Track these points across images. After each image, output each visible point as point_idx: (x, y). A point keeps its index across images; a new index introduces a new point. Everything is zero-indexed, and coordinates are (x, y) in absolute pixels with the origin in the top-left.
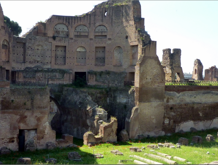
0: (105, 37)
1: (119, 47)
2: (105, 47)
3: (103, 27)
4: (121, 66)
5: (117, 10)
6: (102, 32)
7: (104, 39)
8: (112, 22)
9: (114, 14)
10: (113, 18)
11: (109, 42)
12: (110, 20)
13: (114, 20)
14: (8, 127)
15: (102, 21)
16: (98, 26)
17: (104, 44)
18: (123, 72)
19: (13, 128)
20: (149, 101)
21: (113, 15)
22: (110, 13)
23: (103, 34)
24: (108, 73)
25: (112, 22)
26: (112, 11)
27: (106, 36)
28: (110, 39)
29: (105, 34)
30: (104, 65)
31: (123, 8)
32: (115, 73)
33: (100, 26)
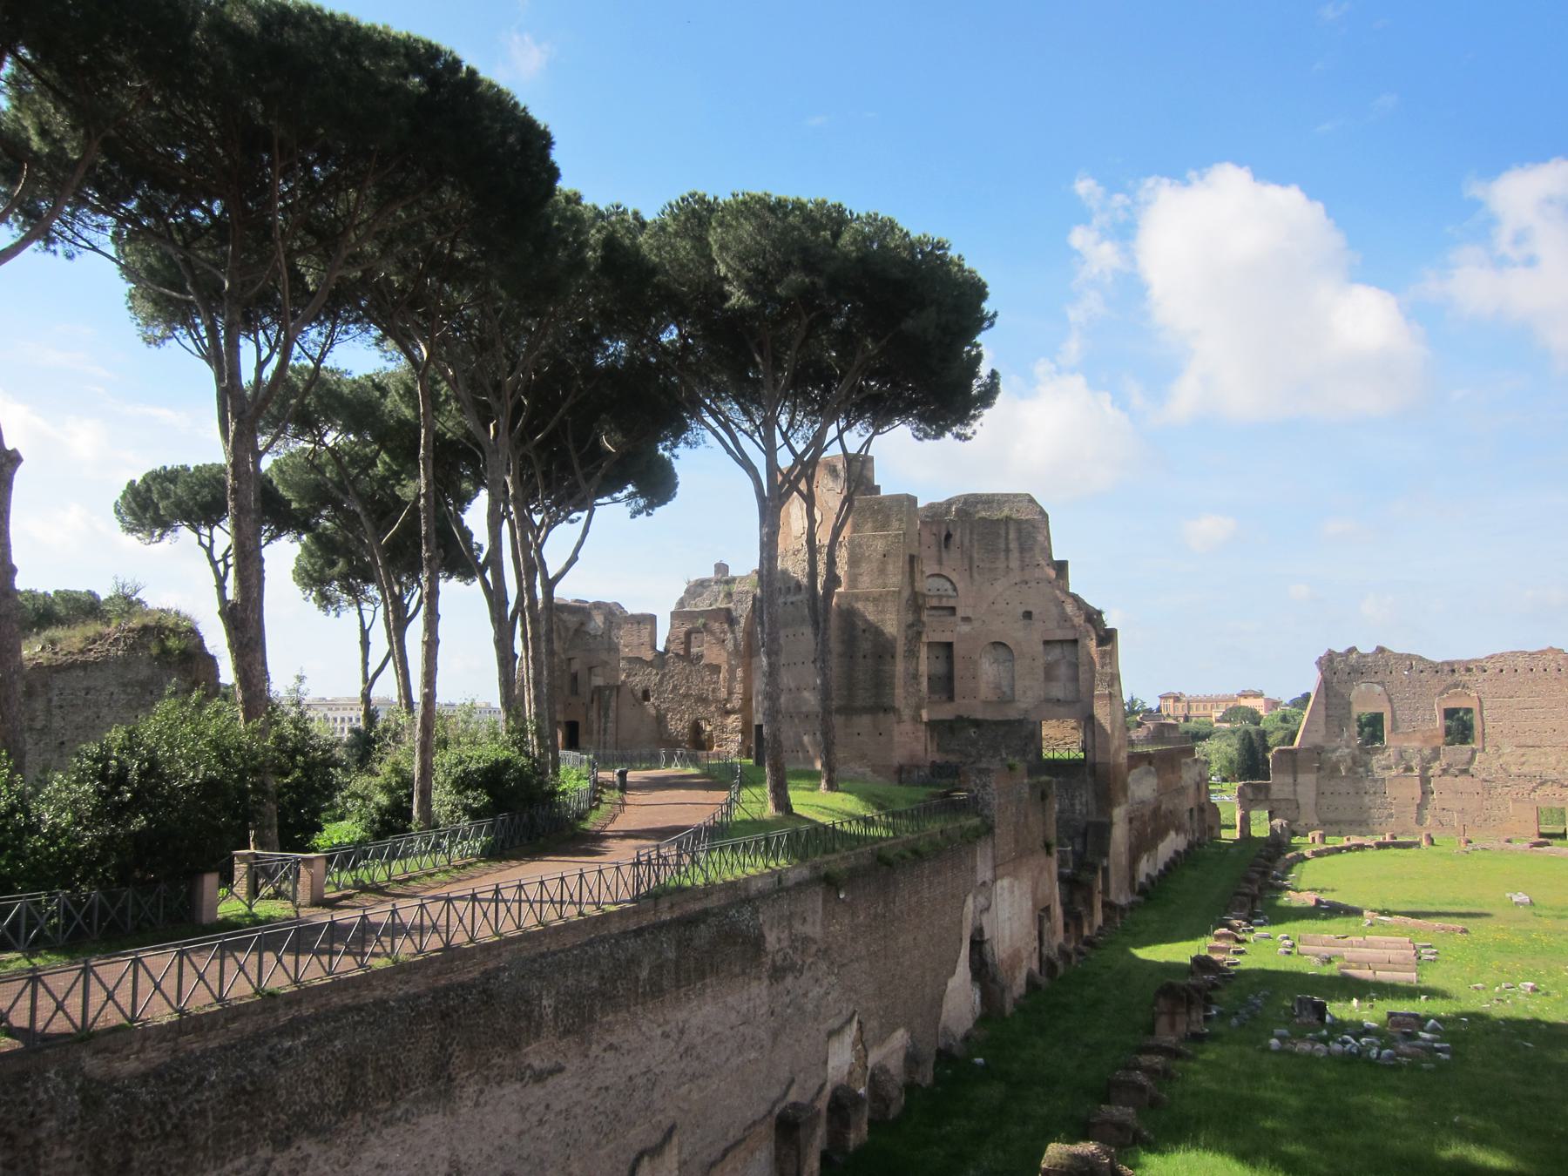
0: (945, 612)
1: (995, 644)
2: (949, 645)
3: (942, 581)
4: (1005, 700)
6: (940, 597)
7: (952, 619)
8: (971, 568)
9: (976, 544)
12: (966, 561)
13: (976, 563)
15: (940, 562)
16: (933, 575)
17: (948, 634)
18: (1020, 722)
19: (1035, 905)
20: (1119, 805)
21: (972, 546)
22: (962, 544)
23: (945, 603)
24: (977, 724)
25: (971, 568)
26: (971, 533)
27: (952, 610)
28: (967, 619)
29: (951, 603)
30: (951, 698)
33: (933, 575)
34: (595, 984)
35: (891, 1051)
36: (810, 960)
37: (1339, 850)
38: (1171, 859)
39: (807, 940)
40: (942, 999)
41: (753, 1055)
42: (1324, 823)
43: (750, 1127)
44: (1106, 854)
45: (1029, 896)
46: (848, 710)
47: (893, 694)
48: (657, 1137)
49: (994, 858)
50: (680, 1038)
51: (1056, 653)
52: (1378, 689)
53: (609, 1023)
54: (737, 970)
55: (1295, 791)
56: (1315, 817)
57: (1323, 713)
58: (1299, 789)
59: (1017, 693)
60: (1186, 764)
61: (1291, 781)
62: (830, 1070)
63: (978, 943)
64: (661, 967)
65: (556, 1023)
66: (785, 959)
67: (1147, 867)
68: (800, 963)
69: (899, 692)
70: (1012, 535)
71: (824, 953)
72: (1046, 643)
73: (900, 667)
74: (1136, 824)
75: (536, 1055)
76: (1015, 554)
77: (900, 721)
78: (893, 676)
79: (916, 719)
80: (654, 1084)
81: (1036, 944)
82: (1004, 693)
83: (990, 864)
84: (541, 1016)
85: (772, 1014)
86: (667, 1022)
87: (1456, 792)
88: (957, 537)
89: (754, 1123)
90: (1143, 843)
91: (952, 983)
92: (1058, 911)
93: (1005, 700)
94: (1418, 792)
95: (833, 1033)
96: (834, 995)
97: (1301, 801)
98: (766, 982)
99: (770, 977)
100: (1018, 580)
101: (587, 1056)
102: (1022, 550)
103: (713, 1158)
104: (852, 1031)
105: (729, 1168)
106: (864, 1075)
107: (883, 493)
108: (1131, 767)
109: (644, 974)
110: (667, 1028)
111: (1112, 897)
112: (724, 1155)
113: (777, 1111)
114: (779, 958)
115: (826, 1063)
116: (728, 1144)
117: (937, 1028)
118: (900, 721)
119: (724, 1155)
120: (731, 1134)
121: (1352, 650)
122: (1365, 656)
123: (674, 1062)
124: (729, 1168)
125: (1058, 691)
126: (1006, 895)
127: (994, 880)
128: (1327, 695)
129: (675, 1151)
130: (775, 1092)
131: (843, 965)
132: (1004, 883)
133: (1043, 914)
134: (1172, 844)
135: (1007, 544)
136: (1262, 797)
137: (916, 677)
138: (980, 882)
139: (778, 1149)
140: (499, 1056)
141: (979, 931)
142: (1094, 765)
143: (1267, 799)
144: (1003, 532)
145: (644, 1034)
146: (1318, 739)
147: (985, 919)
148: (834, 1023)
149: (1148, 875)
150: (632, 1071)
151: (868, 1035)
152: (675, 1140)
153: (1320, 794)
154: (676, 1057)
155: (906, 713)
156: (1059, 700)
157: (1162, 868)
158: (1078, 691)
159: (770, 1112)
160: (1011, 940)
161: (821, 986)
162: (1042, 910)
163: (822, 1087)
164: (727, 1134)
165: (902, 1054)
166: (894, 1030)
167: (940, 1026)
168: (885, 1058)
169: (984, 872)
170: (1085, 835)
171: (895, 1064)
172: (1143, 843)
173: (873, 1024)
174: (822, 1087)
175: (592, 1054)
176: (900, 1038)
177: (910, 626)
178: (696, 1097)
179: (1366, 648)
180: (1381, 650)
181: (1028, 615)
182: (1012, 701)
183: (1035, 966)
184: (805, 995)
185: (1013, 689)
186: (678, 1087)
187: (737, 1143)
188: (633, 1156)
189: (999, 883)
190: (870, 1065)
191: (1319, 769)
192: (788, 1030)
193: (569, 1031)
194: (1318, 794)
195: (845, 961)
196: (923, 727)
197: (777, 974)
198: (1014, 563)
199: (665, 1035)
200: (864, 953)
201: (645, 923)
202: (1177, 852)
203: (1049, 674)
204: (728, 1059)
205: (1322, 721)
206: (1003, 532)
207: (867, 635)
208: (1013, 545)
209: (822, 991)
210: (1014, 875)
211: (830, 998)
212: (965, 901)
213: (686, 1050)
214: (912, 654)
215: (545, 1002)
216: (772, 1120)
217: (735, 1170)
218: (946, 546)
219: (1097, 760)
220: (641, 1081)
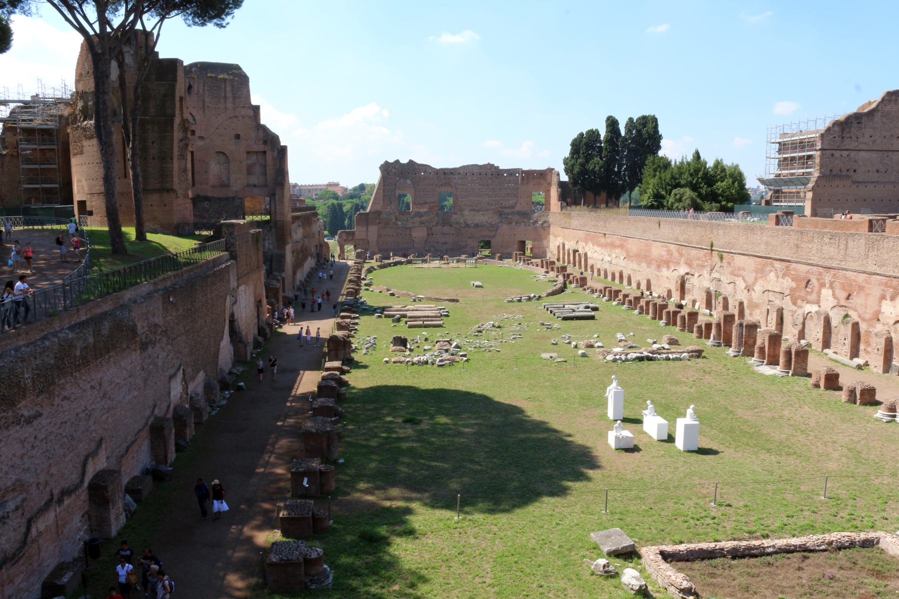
1: (217, 152)
4: (225, 185)
5: (212, 85)
8: (204, 107)
9: (206, 92)
10: (206, 99)
11: (201, 143)
14: (253, 298)
18: (234, 198)
19: (255, 299)
20: (288, 243)
21: (204, 94)
26: (204, 86)
28: (201, 138)
31: (225, 85)
32: (220, 199)
34: (52, 361)
35: (197, 385)
36: (158, 338)
37: (389, 265)
38: (309, 272)
39: (156, 325)
40: (218, 354)
41: (136, 393)
42: (380, 251)
43: (137, 433)
44: (283, 271)
45: (253, 294)
46: (146, 191)
47: (173, 181)
48: (93, 445)
49: (238, 275)
50: (100, 388)
51: (254, 158)
52: (409, 182)
53: (63, 384)
54: (124, 346)
55: (367, 236)
56: (376, 248)
57: (382, 194)
58: (369, 233)
59: (231, 181)
60: (314, 221)
61: (365, 229)
62: (172, 397)
63: (232, 321)
64: (86, 348)
65: (34, 387)
66: (146, 338)
67: (301, 276)
68: (154, 339)
69: (176, 180)
70: (228, 89)
71: (165, 332)
72: (248, 153)
73: (176, 165)
74: (295, 253)
75: (25, 408)
76: (231, 100)
77: (177, 197)
78: (172, 171)
79: (186, 196)
80: (89, 416)
81: (256, 320)
82: (224, 182)
83: (236, 278)
84: (25, 384)
85: (143, 369)
86: (93, 380)
87: (443, 234)
88: (195, 88)
89: (140, 431)
90: (298, 265)
91: (222, 345)
92: (265, 301)
93: (225, 185)
94: (425, 234)
95: (172, 377)
96: (171, 356)
97: (370, 240)
98: (139, 352)
99: (140, 349)
100: (232, 116)
101: (53, 405)
102: (234, 98)
103: (121, 453)
104: (180, 375)
105: (131, 456)
106: (187, 398)
107: (161, 56)
108: (293, 223)
109: (78, 353)
110: (93, 384)
111: (286, 294)
112: (127, 451)
113: (150, 423)
114: (143, 337)
115: (169, 393)
116: (128, 444)
117: (217, 369)
118: (177, 197)
119: (127, 451)
120: (129, 439)
121: (397, 162)
122: (404, 164)
123: (98, 403)
124: (131, 456)
125: (254, 180)
126: (243, 294)
127: (238, 287)
128: (384, 185)
129: (104, 452)
130: (148, 413)
131: (174, 339)
132: (242, 288)
133: (258, 304)
134: (310, 263)
135: (225, 94)
136: (351, 238)
137: (185, 170)
138: (232, 288)
139: (152, 443)
140: (4, 412)
141: (232, 315)
142: (276, 222)
143: (353, 239)
144: (223, 87)
145: (81, 388)
146: (378, 207)
147: (235, 307)
148: (172, 371)
149: (301, 281)
150: (78, 411)
151: (187, 377)
152: (104, 446)
153: (379, 236)
154: (99, 399)
155: (180, 192)
156: (255, 186)
157: (305, 276)
158: (266, 181)
159: (146, 424)
160: (246, 317)
161: (164, 352)
162: (258, 302)
163: (169, 407)
164: (127, 439)
165: (202, 385)
166: (199, 372)
167: (218, 368)
168: (196, 387)
169: (233, 283)
170: (271, 261)
171: (200, 390)
172: (298, 265)
173: (189, 370)
174: (169, 407)
175: (56, 403)
176: (201, 376)
177: (181, 140)
178: (111, 421)
179: (404, 161)
180: (411, 162)
181: (238, 137)
182: (228, 186)
183: (256, 332)
184: (158, 357)
185: (229, 179)
186: (101, 416)
187: (133, 443)
188: (82, 458)
189: (240, 288)
190: (189, 393)
191: (379, 223)
192: (151, 378)
193: (42, 392)
194: (378, 236)
195: (175, 336)
196: (190, 201)
197: (144, 347)
198: (230, 106)
199: (92, 388)
200: (183, 331)
201: (73, 323)
202: (311, 268)
203: (249, 172)
204: (124, 397)
205: (381, 198)
206: (223, 87)
207: (155, 145)
208: (229, 95)
209: (165, 354)
210: (245, 283)
211: (169, 357)
212: (226, 299)
213: (104, 394)
214: (182, 156)
215: (26, 376)
216: (147, 428)
217: (133, 457)
218: (189, 93)
219: (277, 219)
220: (82, 415)
